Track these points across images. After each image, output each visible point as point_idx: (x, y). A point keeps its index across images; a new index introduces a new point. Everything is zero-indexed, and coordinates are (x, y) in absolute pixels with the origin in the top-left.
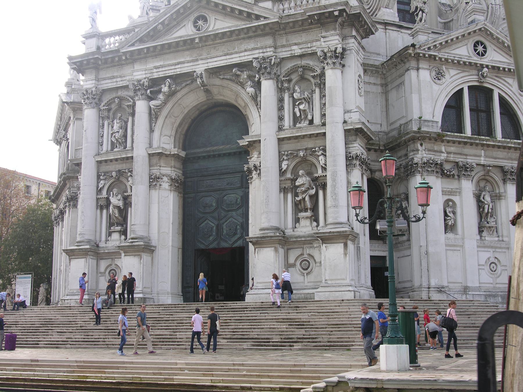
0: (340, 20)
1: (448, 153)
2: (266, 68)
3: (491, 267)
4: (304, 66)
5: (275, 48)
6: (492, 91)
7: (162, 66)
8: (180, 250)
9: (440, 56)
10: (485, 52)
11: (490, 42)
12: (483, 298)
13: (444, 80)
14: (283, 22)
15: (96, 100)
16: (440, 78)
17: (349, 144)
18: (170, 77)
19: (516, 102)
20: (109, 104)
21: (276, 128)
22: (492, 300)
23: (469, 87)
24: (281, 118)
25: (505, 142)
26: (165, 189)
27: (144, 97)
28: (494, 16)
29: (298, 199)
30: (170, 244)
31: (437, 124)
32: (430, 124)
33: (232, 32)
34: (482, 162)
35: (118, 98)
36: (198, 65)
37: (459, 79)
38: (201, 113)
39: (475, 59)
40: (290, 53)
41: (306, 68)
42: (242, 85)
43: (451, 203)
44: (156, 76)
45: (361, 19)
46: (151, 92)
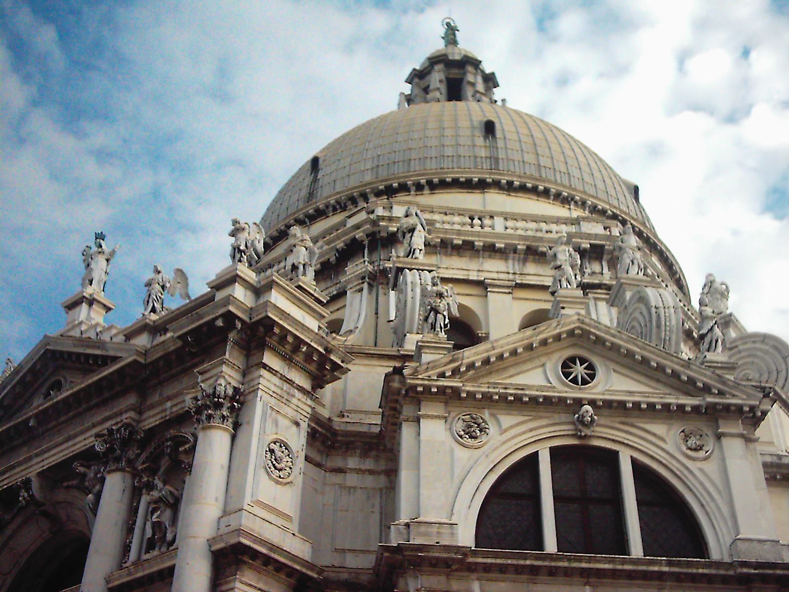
0: (232, 336)
2: (111, 450)
4: (174, 436)
5: (140, 413)
6: (616, 454)
9: (468, 388)
10: (592, 377)
11: (603, 356)
13: (484, 438)
14: (149, 360)
16: (474, 434)
17: (221, 585)
19: (678, 473)
24: (126, 549)
28: (663, 328)
31: (452, 529)
32: (434, 529)
36: (31, 466)
37: (524, 433)
40: (159, 417)
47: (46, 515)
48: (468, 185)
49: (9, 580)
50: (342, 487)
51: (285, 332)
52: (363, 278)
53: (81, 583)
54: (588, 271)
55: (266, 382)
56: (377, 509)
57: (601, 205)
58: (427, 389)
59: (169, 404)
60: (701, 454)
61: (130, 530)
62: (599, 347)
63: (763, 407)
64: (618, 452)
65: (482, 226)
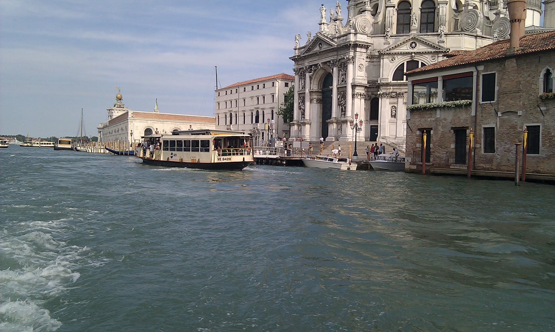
1: (393, 89)
2: (334, 63)
6: (418, 61)
8: (321, 123)
10: (416, 46)
12: (402, 141)
15: (298, 72)
20: (301, 73)
21: (338, 84)
24: (339, 80)
26: (315, 103)
27: (308, 72)
29: (341, 108)
30: (316, 121)
32: (385, 79)
42: (331, 68)
43: (394, 107)
47: (324, 69)
50: (373, 65)
51: (360, 44)
53: (332, 86)
55: (358, 54)
58: (385, 53)
59: (342, 55)
60: (434, 60)
61: (339, 77)
63: (447, 50)
64: (418, 61)
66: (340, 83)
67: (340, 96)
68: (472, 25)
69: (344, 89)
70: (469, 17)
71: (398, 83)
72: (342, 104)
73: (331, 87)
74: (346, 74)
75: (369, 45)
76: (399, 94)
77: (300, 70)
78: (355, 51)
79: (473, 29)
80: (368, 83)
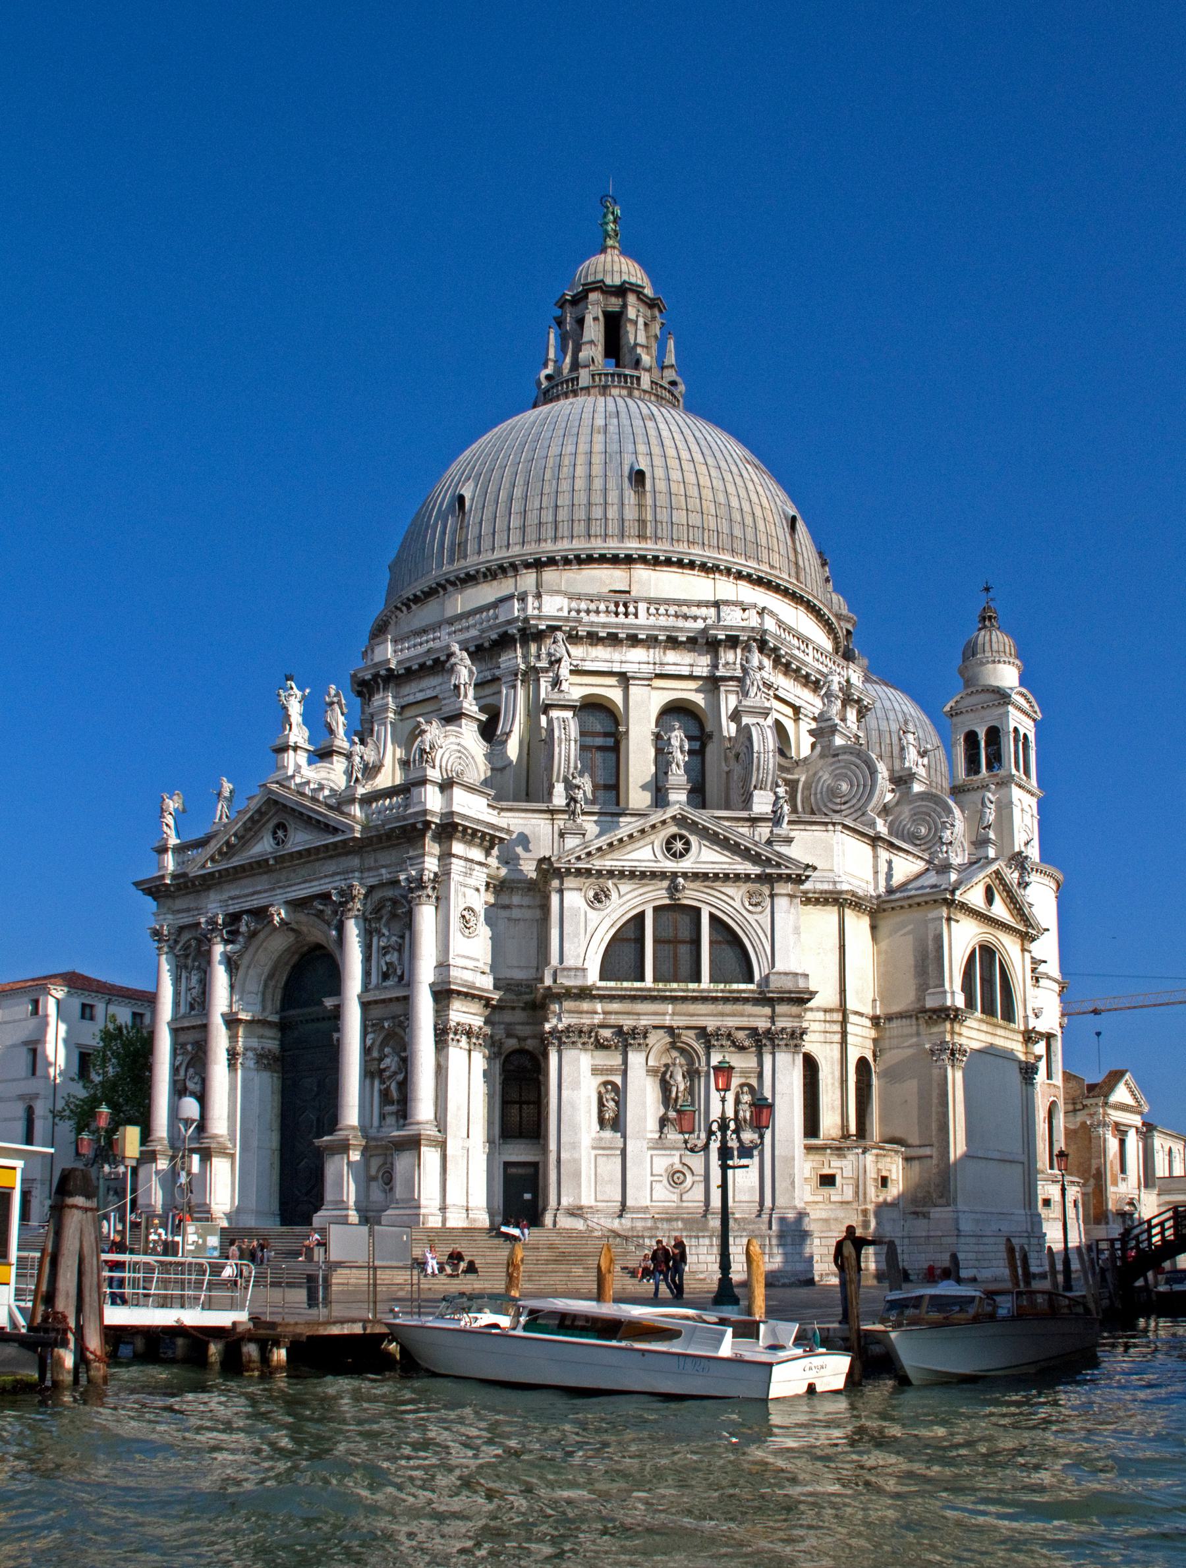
0: (429, 834)
1: (604, 1013)
3: (675, 1177)
7: (238, 897)
8: (277, 1154)
10: (687, 850)
12: (649, 1224)
15: (171, 942)
18: (248, 912)
20: (186, 947)
22: (665, 1226)
23: (656, 909)
25: (710, 991)
33: (308, 850)
34: (667, 1023)
35: (195, 939)
38: (303, 956)
39: (669, 865)
41: (395, 902)
42: (329, 924)
44: (231, 910)
45: (460, 828)
46: (228, 932)
47: (292, 930)
48: (615, 560)
49: (267, 970)
50: (509, 919)
51: (465, 828)
52: (516, 675)
54: (722, 661)
55: (457, 866)
56: (535, 936)
57: (745, 571)
58: (568, 870)
59: (383, 871)
60: (759, 909)
62: (694, 827)
65: (626, 615)
66: (374, 979)
67: (374, 1040)
68: (855, 801)
69: (397, 1009)
70: (840, 774)
71: (622, 989)
72: (384, 1070)
73: (329, 1002)
74: (400, 945)
75: (497, 834)
76: (634, 1032)
77: (179, 935)
78: (446, 856)
79: (860, 813)
80: (496, 987)
